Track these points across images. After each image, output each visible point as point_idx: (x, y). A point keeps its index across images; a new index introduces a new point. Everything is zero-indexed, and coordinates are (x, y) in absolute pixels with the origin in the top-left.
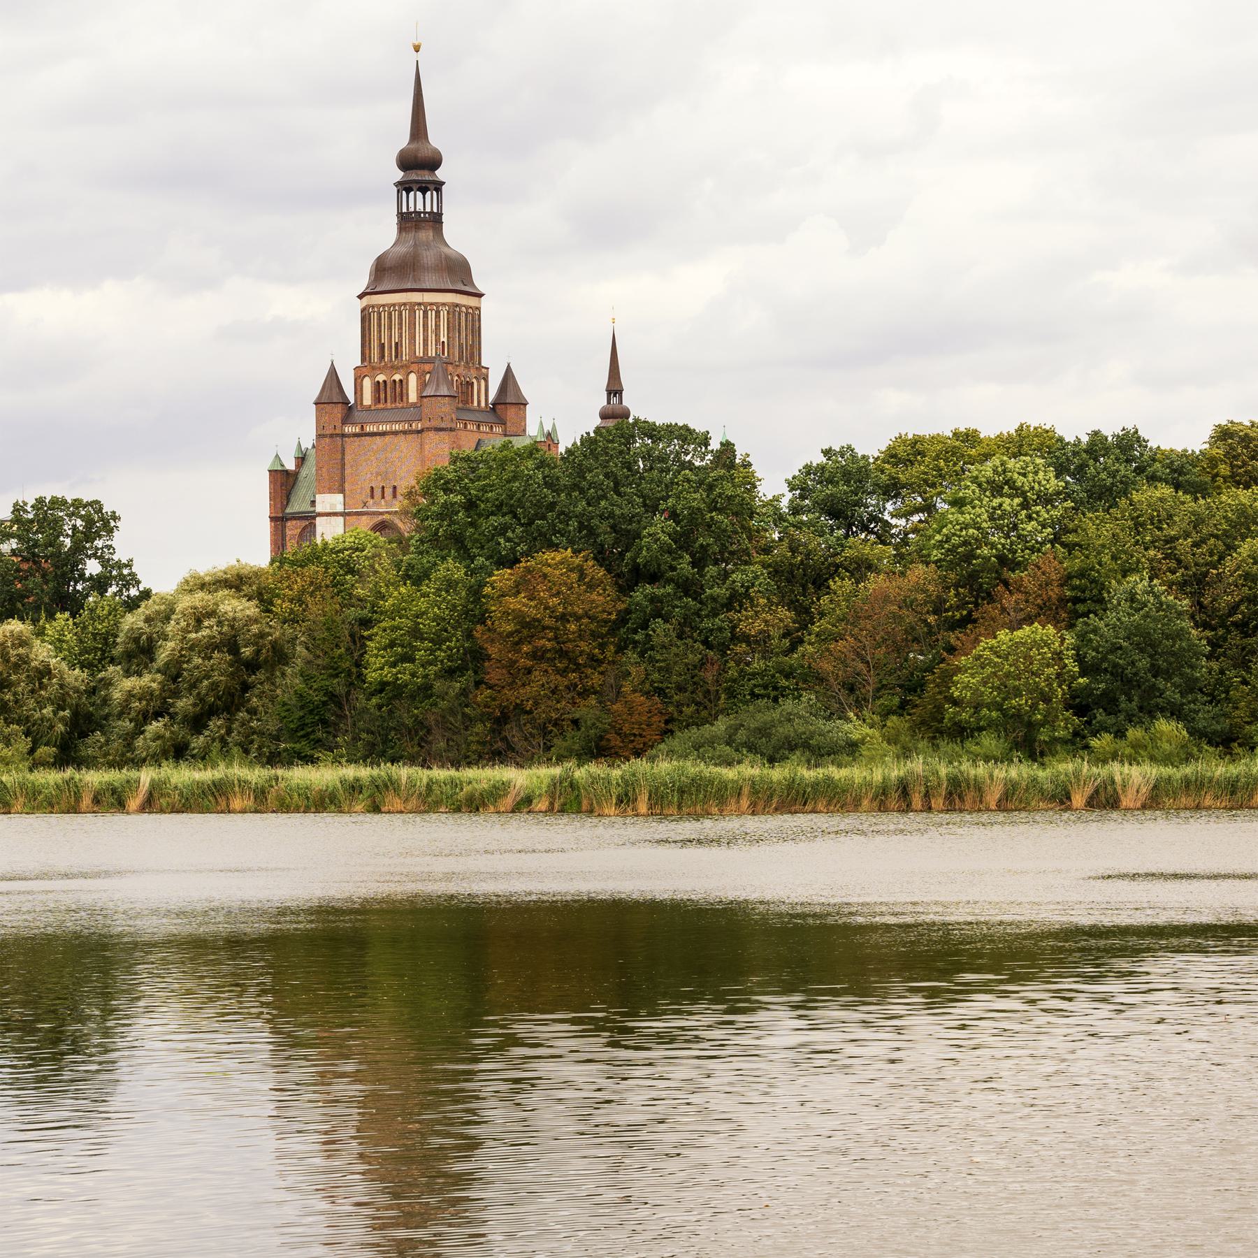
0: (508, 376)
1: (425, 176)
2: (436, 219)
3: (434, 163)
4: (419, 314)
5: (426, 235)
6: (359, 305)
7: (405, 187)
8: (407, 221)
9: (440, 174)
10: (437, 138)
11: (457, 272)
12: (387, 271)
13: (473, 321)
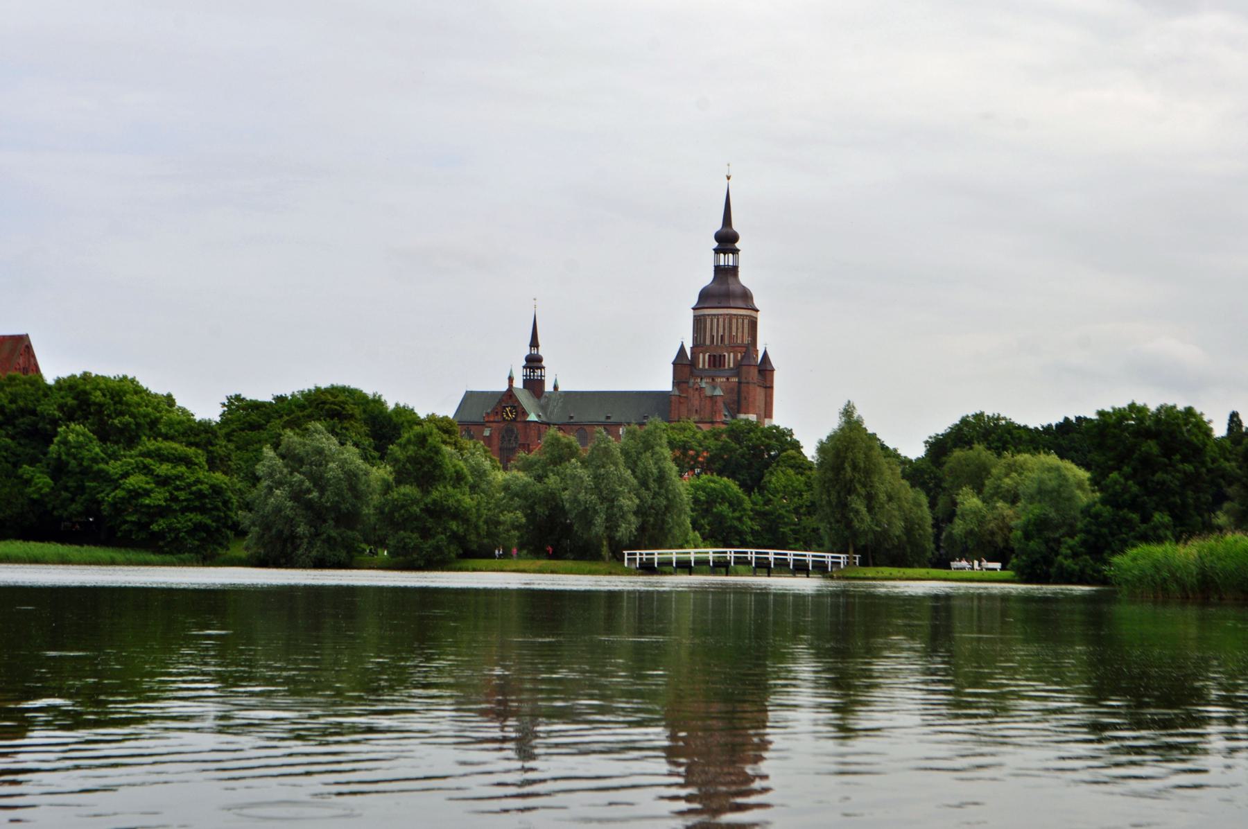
0: (765, 354)
1: (729, 246)
3: (735, 238)
4: (734, 321)
5: (731, 280)
6: (691, 314)
7: (717, 251)
8: (719, 270)
9: (738, 245)
10: (736, 226)
11: (746, 296)
12: (706, 297)
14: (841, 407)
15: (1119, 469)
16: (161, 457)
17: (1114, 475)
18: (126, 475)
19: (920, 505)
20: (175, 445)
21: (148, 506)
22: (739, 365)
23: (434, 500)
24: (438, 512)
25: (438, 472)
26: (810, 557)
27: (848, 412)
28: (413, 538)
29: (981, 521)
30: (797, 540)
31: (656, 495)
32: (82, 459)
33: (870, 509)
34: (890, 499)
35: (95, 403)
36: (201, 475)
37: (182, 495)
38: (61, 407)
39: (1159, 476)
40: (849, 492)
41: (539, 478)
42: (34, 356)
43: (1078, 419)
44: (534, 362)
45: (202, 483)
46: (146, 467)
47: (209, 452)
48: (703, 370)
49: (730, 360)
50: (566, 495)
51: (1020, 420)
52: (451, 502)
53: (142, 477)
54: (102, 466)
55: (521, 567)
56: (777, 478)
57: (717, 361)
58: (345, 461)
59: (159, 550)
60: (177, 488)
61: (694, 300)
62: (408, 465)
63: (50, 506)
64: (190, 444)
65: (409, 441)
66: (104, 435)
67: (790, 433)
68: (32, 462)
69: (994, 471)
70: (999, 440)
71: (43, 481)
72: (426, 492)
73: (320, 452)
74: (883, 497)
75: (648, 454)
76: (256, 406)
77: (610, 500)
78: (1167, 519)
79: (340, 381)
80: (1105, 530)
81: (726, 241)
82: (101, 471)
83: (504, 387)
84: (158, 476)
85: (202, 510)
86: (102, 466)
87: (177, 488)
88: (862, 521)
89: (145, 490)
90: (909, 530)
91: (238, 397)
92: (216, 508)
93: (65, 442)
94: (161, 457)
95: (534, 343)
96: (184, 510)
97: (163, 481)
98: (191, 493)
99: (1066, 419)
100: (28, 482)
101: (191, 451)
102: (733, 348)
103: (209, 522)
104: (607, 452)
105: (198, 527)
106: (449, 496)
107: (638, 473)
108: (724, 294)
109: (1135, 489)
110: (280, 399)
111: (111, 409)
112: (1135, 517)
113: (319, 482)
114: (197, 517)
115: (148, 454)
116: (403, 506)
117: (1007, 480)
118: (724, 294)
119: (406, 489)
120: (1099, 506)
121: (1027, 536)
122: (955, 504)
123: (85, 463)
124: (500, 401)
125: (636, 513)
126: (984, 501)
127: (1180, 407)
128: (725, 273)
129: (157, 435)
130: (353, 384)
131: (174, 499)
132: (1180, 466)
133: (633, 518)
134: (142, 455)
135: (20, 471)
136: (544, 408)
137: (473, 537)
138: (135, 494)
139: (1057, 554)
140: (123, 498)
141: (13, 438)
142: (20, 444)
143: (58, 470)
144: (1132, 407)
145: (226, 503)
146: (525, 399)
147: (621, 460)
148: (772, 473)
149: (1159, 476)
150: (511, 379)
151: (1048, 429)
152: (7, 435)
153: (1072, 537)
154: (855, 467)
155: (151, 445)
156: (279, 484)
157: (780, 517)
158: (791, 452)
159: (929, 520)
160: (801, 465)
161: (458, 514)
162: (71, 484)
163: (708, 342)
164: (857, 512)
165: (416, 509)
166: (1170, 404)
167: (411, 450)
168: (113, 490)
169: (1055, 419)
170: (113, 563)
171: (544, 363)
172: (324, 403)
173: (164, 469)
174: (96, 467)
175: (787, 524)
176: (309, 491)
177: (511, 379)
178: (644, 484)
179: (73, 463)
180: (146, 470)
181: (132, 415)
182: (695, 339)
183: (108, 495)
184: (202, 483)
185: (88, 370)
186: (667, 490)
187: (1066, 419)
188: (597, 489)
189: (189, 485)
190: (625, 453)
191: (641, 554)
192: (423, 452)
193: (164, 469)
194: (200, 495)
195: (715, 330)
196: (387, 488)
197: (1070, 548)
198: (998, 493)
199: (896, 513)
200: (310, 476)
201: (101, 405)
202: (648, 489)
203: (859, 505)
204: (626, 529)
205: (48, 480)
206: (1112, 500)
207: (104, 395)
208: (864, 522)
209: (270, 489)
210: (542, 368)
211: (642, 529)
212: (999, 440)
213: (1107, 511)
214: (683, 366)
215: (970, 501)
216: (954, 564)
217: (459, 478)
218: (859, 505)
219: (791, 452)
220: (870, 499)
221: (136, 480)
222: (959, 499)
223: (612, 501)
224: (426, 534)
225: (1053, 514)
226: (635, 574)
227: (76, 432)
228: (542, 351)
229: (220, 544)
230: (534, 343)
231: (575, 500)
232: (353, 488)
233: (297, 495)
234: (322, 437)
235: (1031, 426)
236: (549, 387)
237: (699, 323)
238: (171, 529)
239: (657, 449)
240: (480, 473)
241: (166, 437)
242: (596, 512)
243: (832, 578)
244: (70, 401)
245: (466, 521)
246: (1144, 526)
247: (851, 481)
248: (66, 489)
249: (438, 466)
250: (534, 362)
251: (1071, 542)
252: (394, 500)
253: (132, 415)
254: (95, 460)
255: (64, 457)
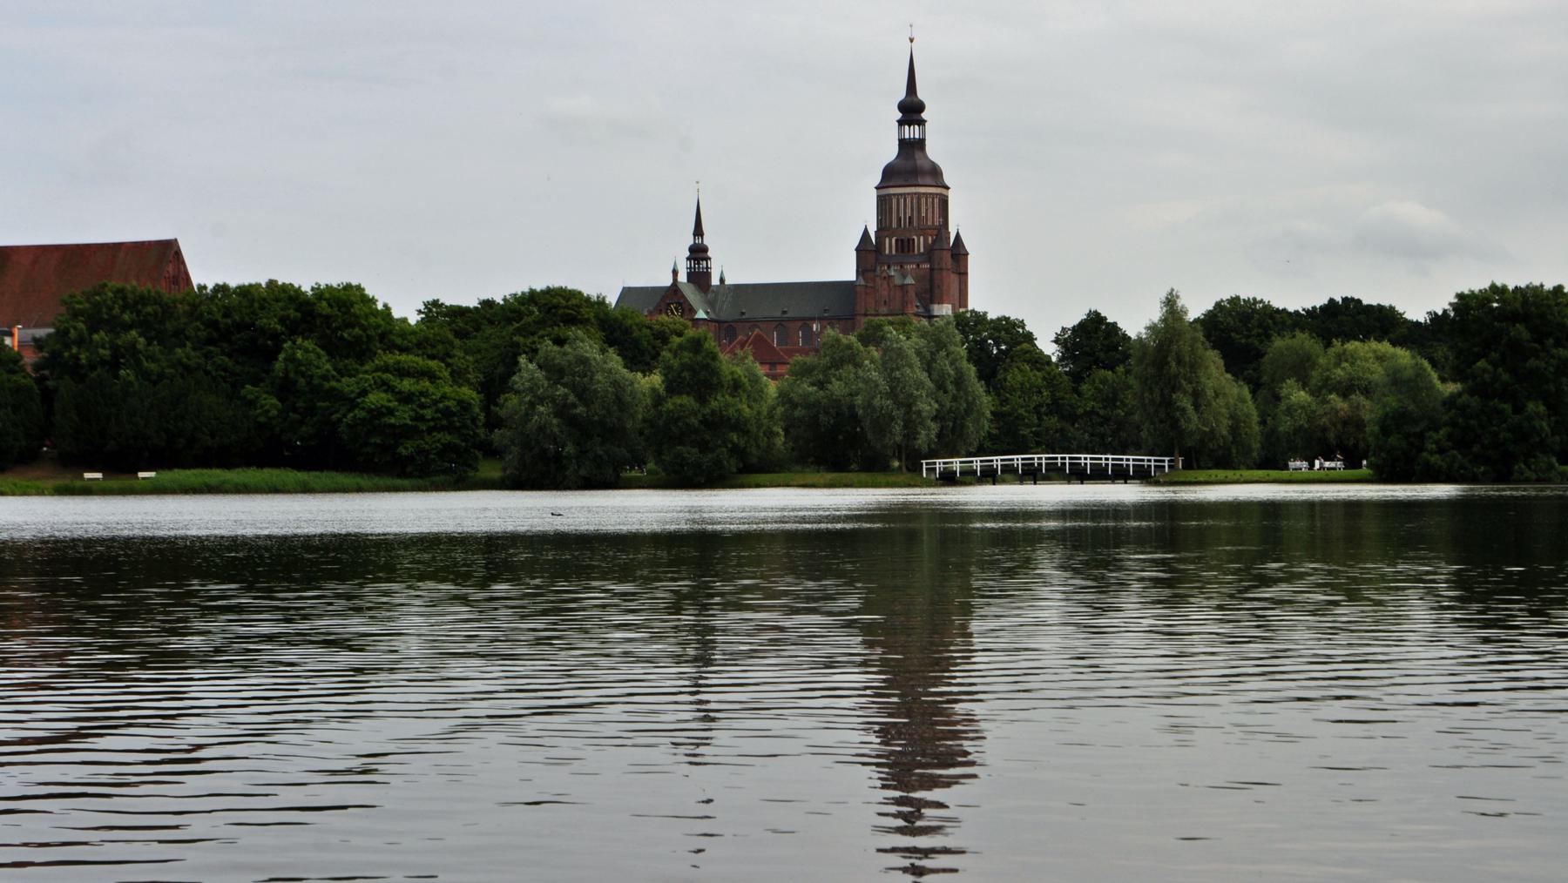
0: (958, 236)
1: (915, 117)
2: (920, 144)
3: (920, 107)
7: (901, 123)
8: (903, 143)
9: (924, 115)
11: (935, 172)
12: (890, 174)
13: (944, 202)
14: (1163, 295)
15: (1484, 356)
16: (403, 373)
17: (1481, 364)
18: (364, 393)
19: (1243, 401)
20: (411, 357)
21: (392, 426)
22: (930, 252)
23: (713, 412)
24: (717, 423)
25: (715, 380)
26: (1129, 460)
27: (1170, 302)
28: (690, 453)
29: (1311, 418)
30: (1038, 444)
31: (955, 399)
32: (311, 377)
33: (1197, 406)
34: (1217, 395)
35: (321, 315)
36: (447, 389)
37: (428, 413)
38: (282, 321)
39: (1532, 363)
40: (1173, 389)
41: (821, 385)
42: (183, 263)
43: (1345, 300)
44: (698, 253)
45: (449, 399)
46: (384, 383)
47: (448, 365)
48: (890, 255)
49: (920, 243)
50: (859, 400)
51: (1278, 304)
52: (731, 411)
53: (383, 395)
54: (334, 383)
55: (810, 482)
56: (1015, 376)
57: (905, 246)
58: (610, 371)
59: (403, 474)
60: (422, 406)
61: (877, 179)
62: (686, 374)
63: (278, 430)
64: (432, 357)
65: (681, 347)
66: (332, 347)
67: (1022, 324)
68: (256, 381)
69: (1322, 361)
70: (1260, 326)
71: (271, 403)
72: (702, 400)
73: (584, 361)
74: (1210, 393)
75: (943, 353)
76: (458, 312)
77: (908, 405)
78: (1542, 408)
79: (556, 282)
80: (1472, 422)
81: (911, 111)
82: (334, 389)
83: (668, 282)
84: (400, 392)
85: (449, 429)
86: (334, 383)
87: (422, 406)
88: (1189, 420)
89: (388, 408)
90: (1234, 430)
91: (435, 303)
92: (466, 427)
93: (291, 359)
94: (403, 373)
95: (698, 231)
96: (430, 431)
97: (406, 398)
98: (437, 411)
99: (1332, 301)
100: (251, 404)
101: (433, 364)
102: (923, 231)
103: (457, 441)
104: (900, 353)
105: (448, 449)
106: (727, 405)
107: (935, 376)
108: (911, 170)
109: (1506, 377)
110: (488, 304)
111: (340, 318)
112: (1507, 407)
113: (584, 394)
114: (447, 438)
115: (386, 369)
116: (679, 419)
117: (1339, 371)
118: (911, 170)
119: (686, 400)
120: (1465, 397)
121: (1385, 431)
122: (1278, 398)
123: (316, 382)
124: (663, 299)
125: (934, 419)
126: (1312, 393)
127: (1549, 286)
128: (912, 148)
129: (392, 347)
130: (571, 284)
131: (421, 418)
132: (1554, 351)
133: (933, 425)
134: (377, 369)
135: (243, 392)
136: (711, 304)
137: (754, 450)
138: (378, 413)
139: (1421, 449)
140: (364, 419)
141: (230, 356)
142: (237, 362)
143: (285, 389)
144: (1493, 287)
145: (474, 420)
146: (691, 294)
147: (916, 361)
148: (1006, 370)
149: (1532, 363)
150: (675, 273)
151: (1311, 313)
152: (223, 353)
153: (1437, 431)
154: (1179, 362)
155: (390, 358)
156: (541, 400)
157: (1020, 418)
158: (1025, 346)
159: (1255, 418)
160: (1040, 360)
161: (739, 426)
162: (300, 404)
163: (894, 225)
164: (1184, 410)
165: (694, 421)
166: (1536, 283)
167: (687, 356)
168: (350, 411)
169: (1320, 301)
170: (359, 490)
171: (709, 254)
172: (556, 307)
173: (407, 385)
174: (327, 385)
175: (1028, 426)
176: (574, 406)
177: (675, 273)
178: (941, 386)
179: (302, 381)
180: (386, 386)
181: (364, 329)
182: (879, 222)
183: (345, 416)
184: (449, 399)
185: (273, 277)
186: (967, 393)
187: (1332, 301)
188: (892, 394)
189: (435, 402)
190: (918, 353)
191: (939, 464)
192: (699, 358)
193: (407, 385)
194: (447, 413)
195: (903, 211)
196: (658, 400)
197: (1437, 443)
198: (1327, 385)
199: (1224, 410)
200: (573, 387)
201: (328, 317)
202: (946, 392)
203: (1186, 402)
204: (927, 434)
205: (275, 401)
206: (1481, 390)
207: (330, 306)
208: (1192, 421)
209: (532, 405)
210: (707, 259)
211: (940, 435)
212: (1260, 326)
213: (1475, 402)
214: (867, 252)
215: (1300, 396)
216: (1292, 464)
217: (736, 386)
218: (1186, 402)
219: (1025, 346)
220: (1197, 396)
221: (376, 398)
222: (1284, 392)
223: (909, 406)
224: (704, 447)
225: (1411, 407)
226: (935, 486)
227: (305, 348)
228: (707, 240)
229: (470, 466)
230: (698, 231)
231: (869, 406)
232: (619, 400)
233: (562, 411)
234: (588, 346)
235: (1291, 309)
236: (715, 281)
237: (883, 204)
238: (420, 451)
239: (952, 348)
240: (755, 380)
241: (403, 350)
242: (892, 419)
243: (1157, 483)
244: (293, 313)
245: (746, 432)
246: (1517, 418)
247: (1176, 376)
248: (295, 410)
249: (715, 373)
250: (698, 253)
251: (1436, 436)
252: (669, 411)
253: (364, 329)
254: (325, 378)
255: (292, 375)
